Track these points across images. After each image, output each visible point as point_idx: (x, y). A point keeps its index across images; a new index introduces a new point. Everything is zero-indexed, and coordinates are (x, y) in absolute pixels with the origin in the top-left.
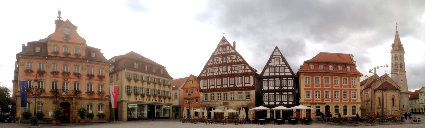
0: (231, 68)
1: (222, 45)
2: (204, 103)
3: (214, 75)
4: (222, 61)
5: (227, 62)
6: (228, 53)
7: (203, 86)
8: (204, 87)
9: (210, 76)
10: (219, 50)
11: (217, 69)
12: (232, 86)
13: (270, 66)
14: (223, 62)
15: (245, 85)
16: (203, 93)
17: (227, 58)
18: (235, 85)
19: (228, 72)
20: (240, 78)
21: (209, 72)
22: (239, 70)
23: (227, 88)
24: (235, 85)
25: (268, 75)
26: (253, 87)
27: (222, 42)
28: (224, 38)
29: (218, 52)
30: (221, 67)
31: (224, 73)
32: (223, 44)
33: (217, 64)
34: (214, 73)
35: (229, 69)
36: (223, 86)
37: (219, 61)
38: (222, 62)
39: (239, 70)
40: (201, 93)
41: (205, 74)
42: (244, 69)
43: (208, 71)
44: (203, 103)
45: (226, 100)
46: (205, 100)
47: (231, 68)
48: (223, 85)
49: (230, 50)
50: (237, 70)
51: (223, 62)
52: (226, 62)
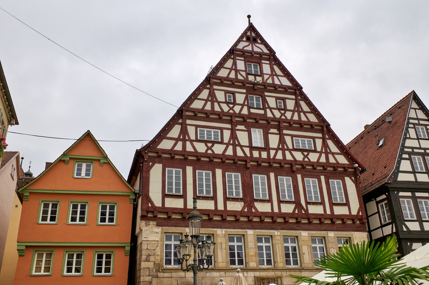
0: (282, 141)
1: (245, 48)
2: (166, 275)
3: (216, 152)
4: (249, 108)
5: (266, 112)
6: (270, 85)
7: (165, 196)
8: (167, 200)
9: (196, 154)
10: (235, 64)
11: (227, 134)
12: (287, 209)
13: (410, 150)
14: (252, 111)
15: (332, 210)
16: (158, 225)
17: (265, 101)
18: (297, 203)
19: (272, 153)
20: (311, 182)
21: (193, 137)
22: (309, 151)
23: (272, 215)
24: (297, 203)
25: (410, 178)
26: (360, 220)
27: (244, 39)
28: (251, 28)
29: (233, 72)
30: (243, 127)
31: (256, 154)
32: (249, 48)
33: (227, 114)
34: (214, 143)
35: (274, 140)
36: (257, 204)
37: (235, 103)
38: (245, 108)
39: (309, 151)
40: (147, 225)
41: (177, 140)
42: (324, 151)
43: (191, 131)
44: (161, 274)
45: (265, 266)
46: (168, 262)
47: (282, 141)
48: (257, 201)
49: (277, 76)
50: (302, 151)
51: (252, 111)
52: (262, 112)
